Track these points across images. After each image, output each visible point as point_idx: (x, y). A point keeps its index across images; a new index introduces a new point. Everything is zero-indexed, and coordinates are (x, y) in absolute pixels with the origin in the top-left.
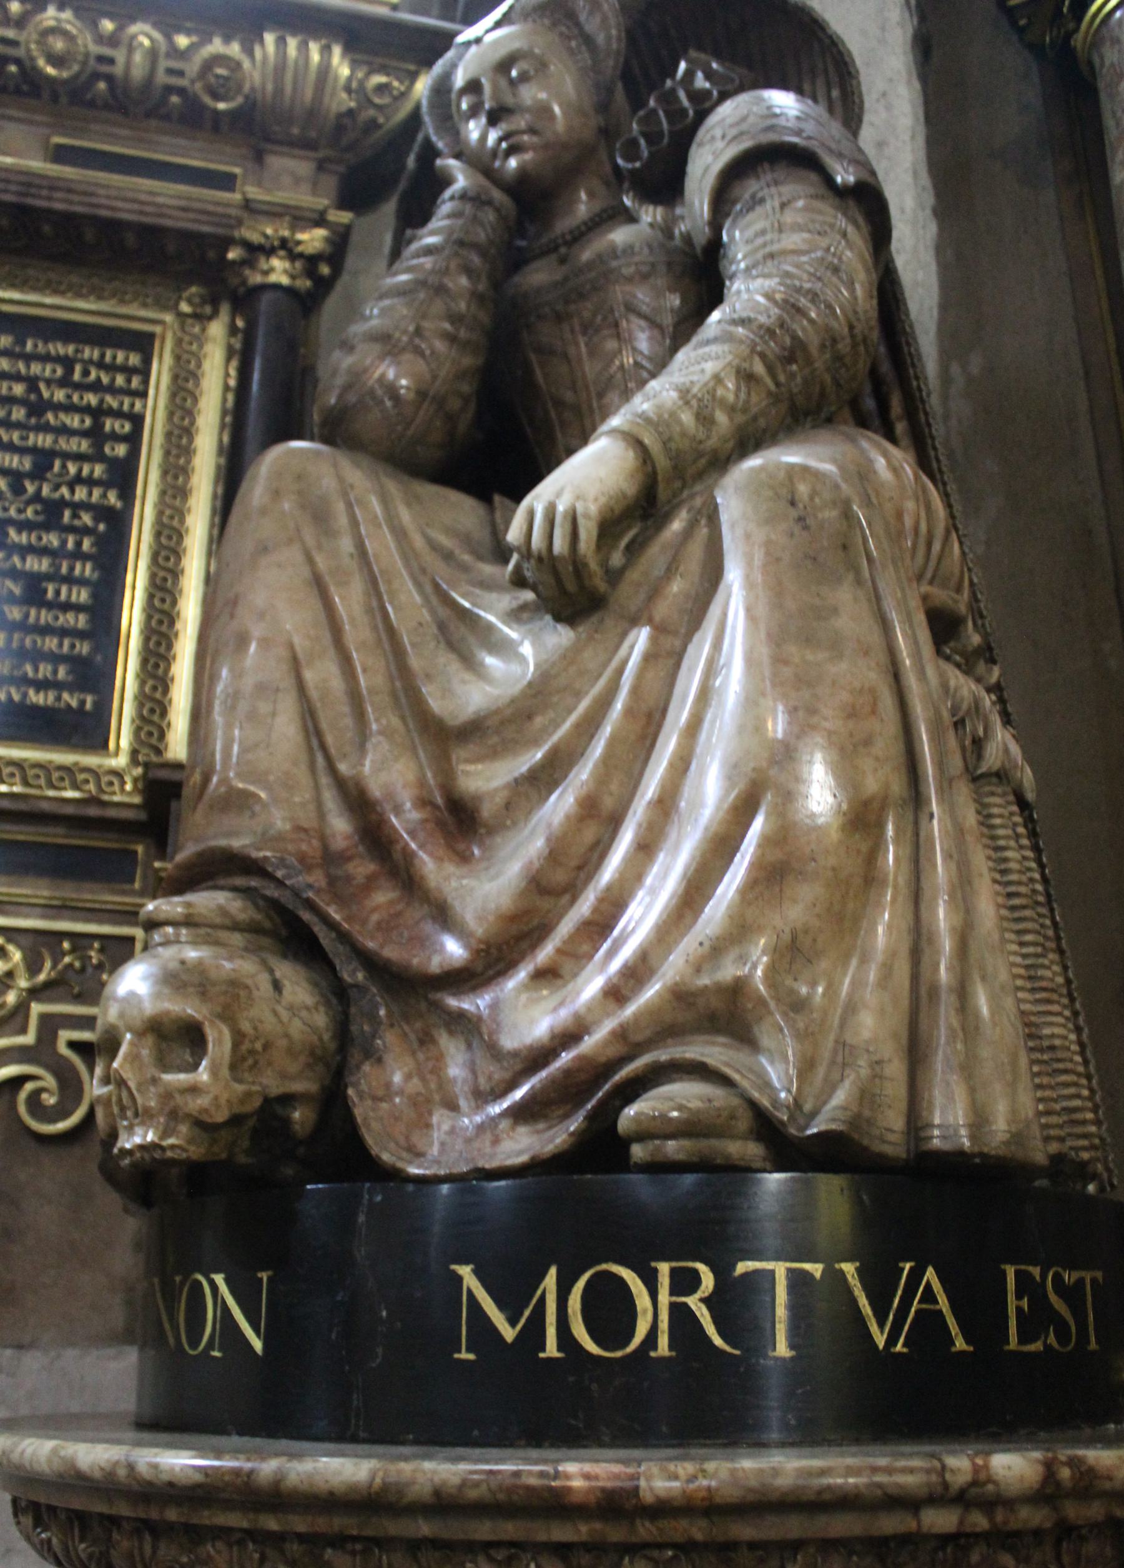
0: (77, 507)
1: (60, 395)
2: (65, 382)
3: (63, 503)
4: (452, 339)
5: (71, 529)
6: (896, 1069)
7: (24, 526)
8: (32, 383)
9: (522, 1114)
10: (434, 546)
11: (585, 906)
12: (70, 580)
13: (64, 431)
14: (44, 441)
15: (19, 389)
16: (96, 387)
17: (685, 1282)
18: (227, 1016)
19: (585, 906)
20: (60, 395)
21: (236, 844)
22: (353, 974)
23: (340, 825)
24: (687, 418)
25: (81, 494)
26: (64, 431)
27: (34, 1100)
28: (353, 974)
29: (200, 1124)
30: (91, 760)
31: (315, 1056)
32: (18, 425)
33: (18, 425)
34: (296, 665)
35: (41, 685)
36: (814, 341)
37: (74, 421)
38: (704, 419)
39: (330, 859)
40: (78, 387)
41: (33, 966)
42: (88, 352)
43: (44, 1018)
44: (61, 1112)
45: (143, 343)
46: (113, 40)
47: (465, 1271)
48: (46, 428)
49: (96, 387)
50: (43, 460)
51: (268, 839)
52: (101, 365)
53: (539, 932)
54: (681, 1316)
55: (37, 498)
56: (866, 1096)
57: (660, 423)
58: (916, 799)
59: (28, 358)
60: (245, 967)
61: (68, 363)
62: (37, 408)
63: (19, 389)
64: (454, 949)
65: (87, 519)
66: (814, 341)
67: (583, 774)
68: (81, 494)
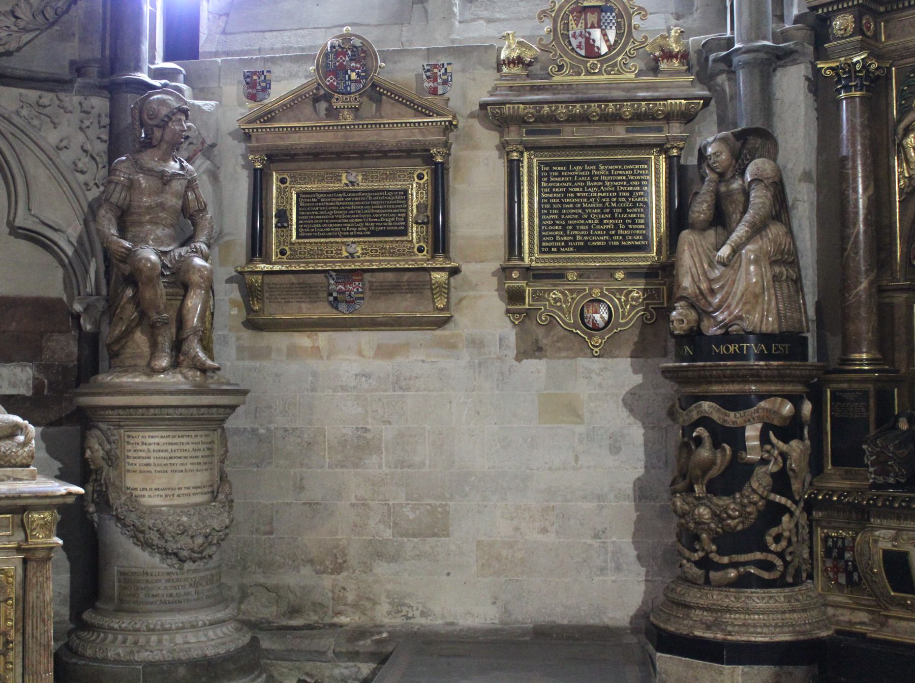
0: (639, 202)
1: (632, 178)
2: (633, 175)
3: (637, 202)
4: (709, 210)
5: (638, 207)
6: (759, 324)
7: (630, 208)
8: (626, 175)
9: (719, 328)
10: (708, 248)
11: (726, 305)
12: (640, 218)
13: (634, 186)
14: (631, 188)
15: (624, 178)
16: (639, 174)
17: (735, 346)
18: (686, 318)
19: (726, 305)
20: (632, 178)
21: (685, 295)
22: (700, 311)
23: (697, 291)
24: (738, 240)
25: (639, 199)
26: (634, 186)
27: (646, 317)
28: (700, 311)
29: (685, 331)
30: (648, 255)
31: (696, 321)
32: (625, 186)
33: (625, 186)
34: (690, 269)
35: (637, 240)
36: (758, 223)
37: (636, 183)
38: (741, 240)
39: (696, 296)
40: (636, 175)
41: (644, 295)
42: (637, 167)
43: (647, 304)
44: (649, 320)
45: (646, 162)
46: (637, 109)
47: (713, 346)
48: (630, 186)
49: (639, 174)
50: (631, 192)
51: (689, 294)
52: (640, 169)
53: (722, 306)
54: (735, 350)
55: (631, 201)
56: (755, 327)
57: (735, 242)
58: (764, 293)
59: (625, 170)
60: (688, 312)
61: (632, 170)
62: (629, 181)
63: (624, 178)
64: (711, 309)
65: (641, 205)
66: (758, 223)
67: (726, 289)
68: (639, 199)
